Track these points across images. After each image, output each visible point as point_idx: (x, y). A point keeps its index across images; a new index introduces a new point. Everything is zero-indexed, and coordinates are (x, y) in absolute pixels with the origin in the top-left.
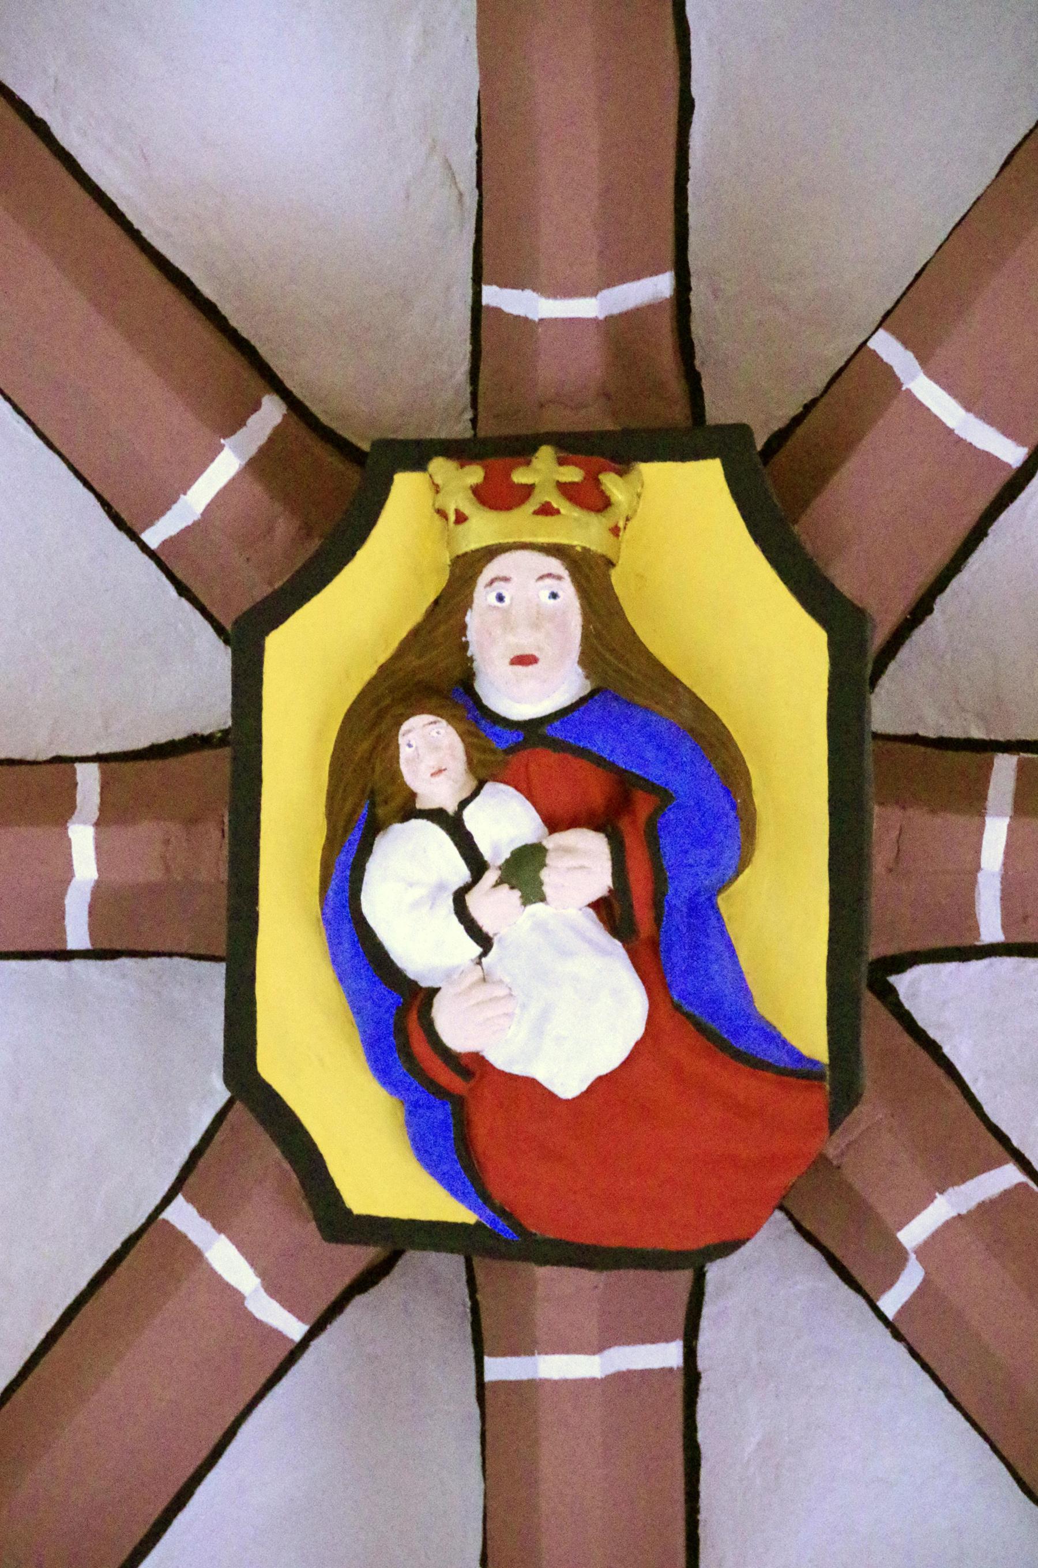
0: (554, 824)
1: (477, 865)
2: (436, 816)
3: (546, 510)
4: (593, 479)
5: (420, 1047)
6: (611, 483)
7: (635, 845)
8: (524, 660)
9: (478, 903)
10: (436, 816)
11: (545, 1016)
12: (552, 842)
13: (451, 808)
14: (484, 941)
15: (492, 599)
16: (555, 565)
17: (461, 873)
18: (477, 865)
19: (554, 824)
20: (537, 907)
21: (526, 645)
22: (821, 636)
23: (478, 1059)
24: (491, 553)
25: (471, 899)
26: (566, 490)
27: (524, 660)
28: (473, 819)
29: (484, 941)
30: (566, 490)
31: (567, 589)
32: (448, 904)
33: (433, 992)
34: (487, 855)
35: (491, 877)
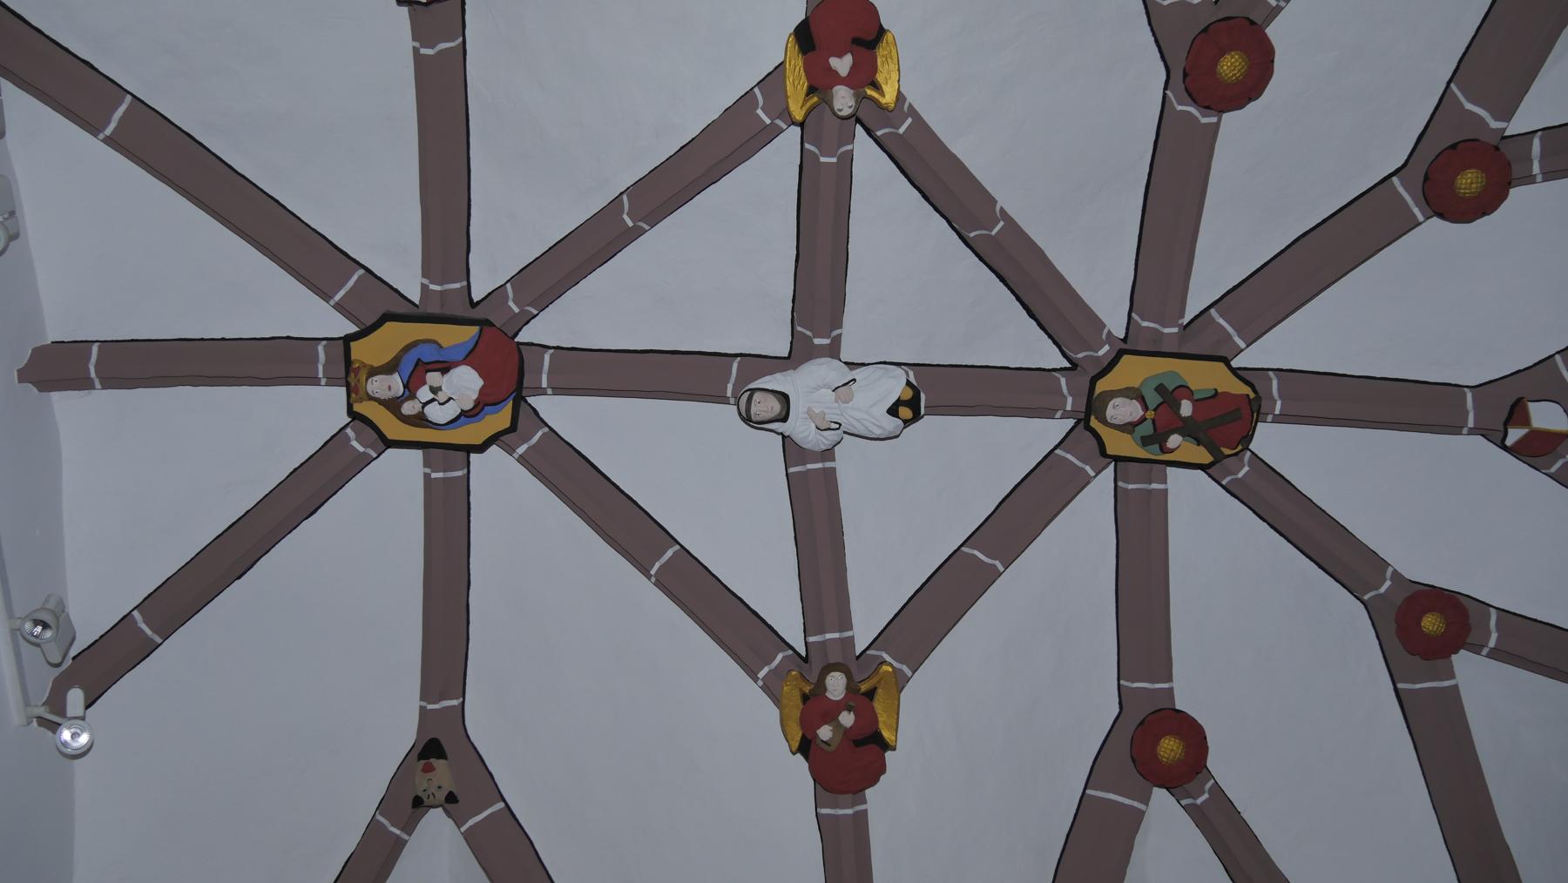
1: (433, 400)
2: (423, 408)
3: (359, 380)
5: (471, 413)
7: (429, 367)
8: (390, 388)
10: (423, 408)
14: (450, 399)
16: (370, 380)
17: (436, 403)
18: (433, 400)
20: (443, 388)
21: (386, 387)
22: (388, 323)
23: (475, 401)
25: (441, 402)
26: (356, 376)
27: (390, 388)
29: (450, 399)
30: (356, 376)
31: (375, 378)
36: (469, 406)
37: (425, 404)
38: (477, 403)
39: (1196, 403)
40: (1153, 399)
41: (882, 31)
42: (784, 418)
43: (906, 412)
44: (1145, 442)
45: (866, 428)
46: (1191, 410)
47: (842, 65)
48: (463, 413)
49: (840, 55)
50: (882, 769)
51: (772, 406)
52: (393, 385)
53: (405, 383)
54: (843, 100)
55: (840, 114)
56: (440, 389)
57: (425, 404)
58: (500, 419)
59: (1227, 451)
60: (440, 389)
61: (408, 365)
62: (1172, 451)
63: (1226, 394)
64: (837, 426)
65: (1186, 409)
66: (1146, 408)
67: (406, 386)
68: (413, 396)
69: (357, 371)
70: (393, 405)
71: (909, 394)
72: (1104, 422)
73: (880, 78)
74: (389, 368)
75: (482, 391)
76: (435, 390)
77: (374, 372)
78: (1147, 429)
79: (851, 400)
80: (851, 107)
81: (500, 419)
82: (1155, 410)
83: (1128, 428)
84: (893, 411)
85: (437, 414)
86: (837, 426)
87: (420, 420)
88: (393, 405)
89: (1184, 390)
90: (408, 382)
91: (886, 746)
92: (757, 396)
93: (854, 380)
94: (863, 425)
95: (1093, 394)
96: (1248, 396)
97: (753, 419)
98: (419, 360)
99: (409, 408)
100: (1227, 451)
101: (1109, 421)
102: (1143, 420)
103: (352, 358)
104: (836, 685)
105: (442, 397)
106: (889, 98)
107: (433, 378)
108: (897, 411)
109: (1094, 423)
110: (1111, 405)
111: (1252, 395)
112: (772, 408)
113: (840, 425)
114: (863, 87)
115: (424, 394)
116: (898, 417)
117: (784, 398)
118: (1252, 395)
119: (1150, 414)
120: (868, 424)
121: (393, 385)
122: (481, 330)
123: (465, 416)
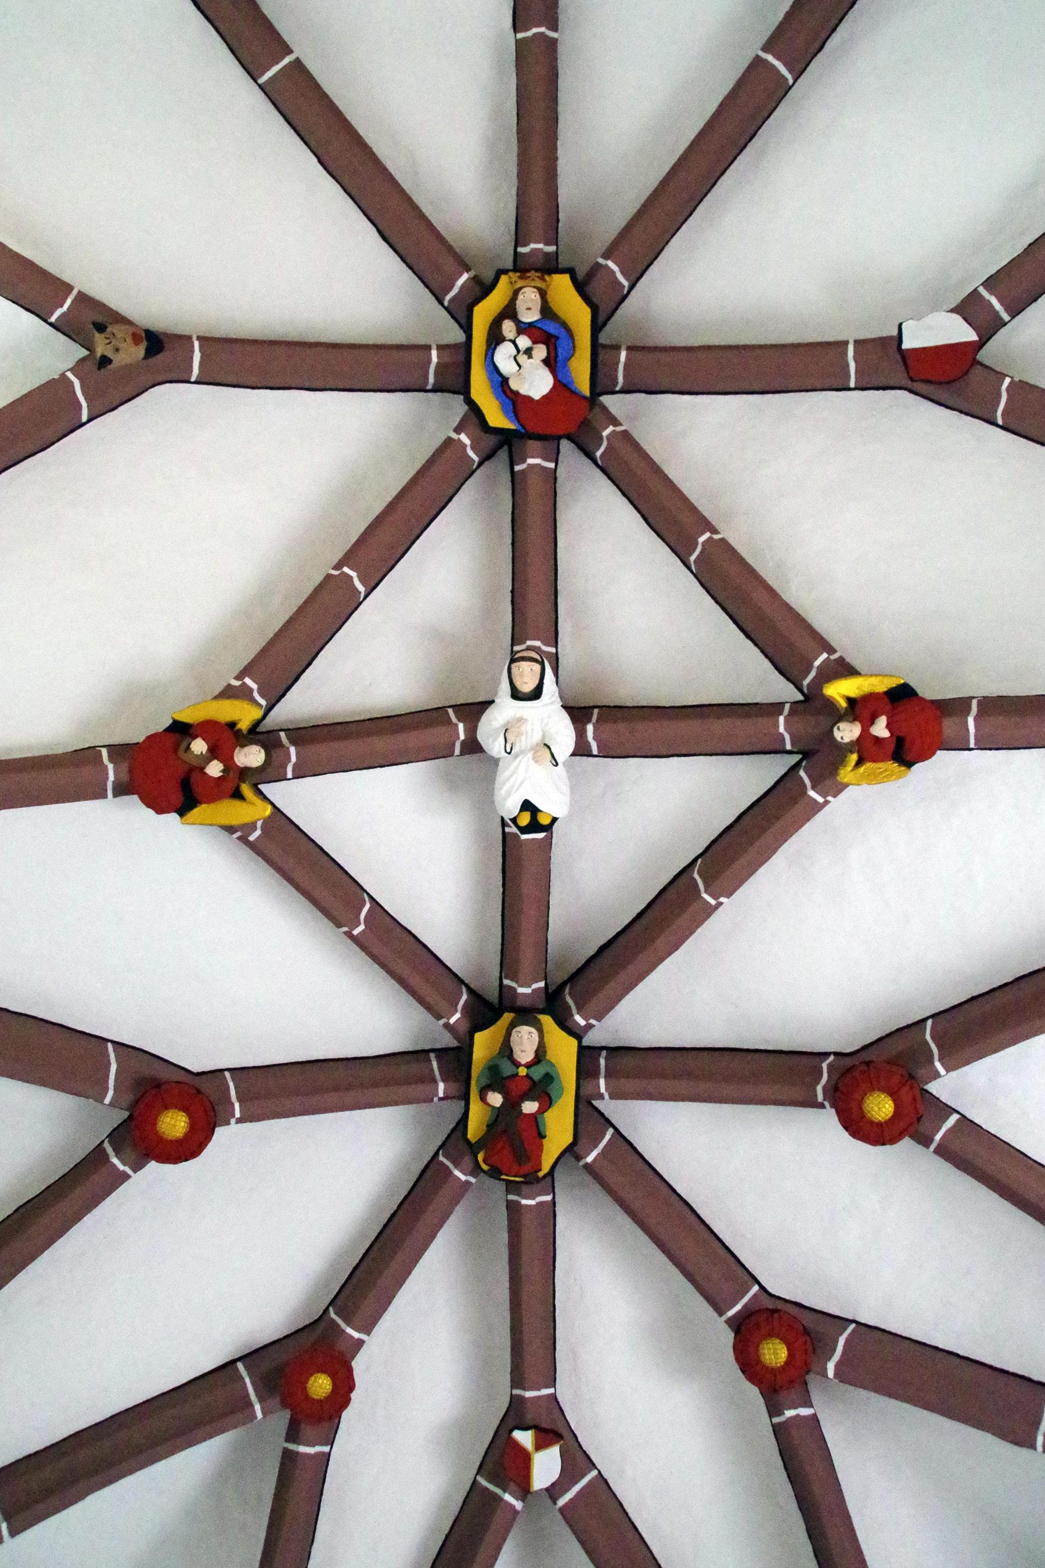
0: (535, 342)
1: (518, 351)
2: (510, 341)
3: (533, 280)
4: (543, 276)
6: (547, 277)
7: (552, 348)
8: (529, 309)
9: (519, 358)
10: (510, 341)
11: (532, 383)
12: (535, 346)
13: (513, 339)
14: (520, 366)
15: (522, 296)
16: (535, 290)
17: (515, 352)
18: (518, 351)
19: (535, 342)
20: (531, 360)
21: (530, 305)
24: (520, 289)
26: (538, 277)
27: (529, 309)
28: (518, 341)
29: (520, 366)
31: (538, 295)
32: (513, 358)
33: (508, 378)
34: (520, 348)
35: (521, 353)
36: (514, 385)
37: (514, 342)
38: (517, 394)
39: (534, 1118)
40: (537, 1073)
41: (909, 764)
42: (516, 695)
43: (525, 819)
44: (493, 1069)
45: (508, 779)
46: (528, 1112)
47: (880, 729)
48: (505, 380)
49: (888, 726)
50: (160, 810)
51: (527, 685)
52: (529, 312)
53: (535, 324)
54: (847, 732)
55: (835, 729)
56: (530, 357)
57: (514, 342)
58: (497, 417)
59: (480, 1157)
60: (530, 357)
61: (551, 328)
62: (483, 1099)
63: (540, 1148)
64: (508, 750)
65: (530, 1107)
66: (528, 1066)
67: (530, 324)
68: (520, 332)
69: (543, 279)
70: (509, 312)
71: (544, 821)
72: (513, 1025)
73: (868, 766)
74: (547, 311)
75: (528, 399)
76: (528, 352)
77: (543, 294)
78: (507, 1069)
79: (536, 762)
80: (842, 738)
81: (497, 417)
82: (527, 1076)
83: (506, 1050)
84: (527, 806)
85: (504, 358)
86: (508, 750)
87: (495, 338)
88: (509, 312)
89: (547, 1102)
90: (535, 327)
91: (182, 812)
92: (537, 667)
93: (557, 764)
94: (511, 776)
95: (538, 1013)
96: (540, 1170)
97: (513, 666)
98: (557, 338)
99: (508, 328)
100: (480, 1157)
101: (514, 1030)
102: (517, 1065)
103: (553, 275)
104: (252, 757)
105: (522, 358)
106: (846, 774)
108: (527, 810)
109: (508, 1017)
110: (533, 1030)
111: (541, 1174)
112: (526, 683)
113: (509, 753)
114: (858, 752)
115: (524, 342)
116: (521, 810)
117: (536, 694)
118: (541, 1174)
119: (523, 1071)
120: (512, 780)
121: (529, 312)
122: (584, 398)
123: (502, 382)
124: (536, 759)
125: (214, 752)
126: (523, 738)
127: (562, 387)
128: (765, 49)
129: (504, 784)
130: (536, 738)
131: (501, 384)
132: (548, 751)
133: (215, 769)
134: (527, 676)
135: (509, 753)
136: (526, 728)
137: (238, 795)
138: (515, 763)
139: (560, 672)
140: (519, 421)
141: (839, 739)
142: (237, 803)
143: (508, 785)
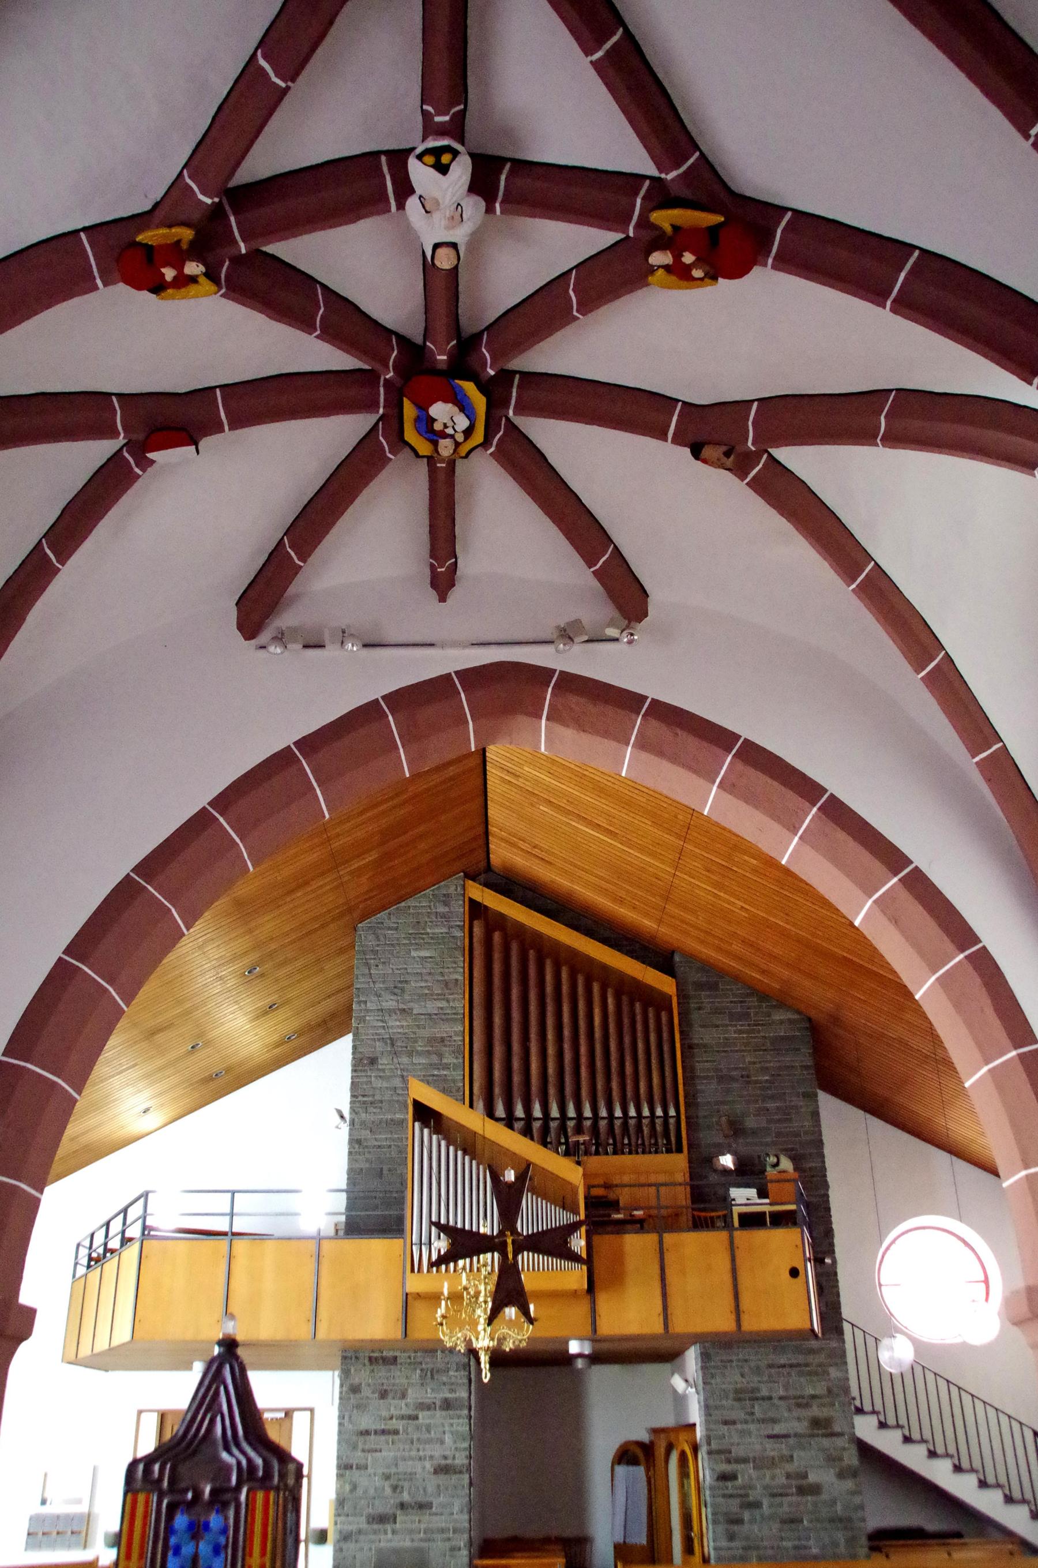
42: (454, 246)
43: (445, 159)
49: (164, 275)
57: (455, 431)
71: (430, 159)
76: (445, 426)
84: (443, 169)
86: (459, 207)
87: (468, 432)
88: (457, 445)
99: (460, 438)
107: (438, 427)
113: (459, 204)
115: (450, 431)
117: (436, 246)
121: (443, 443)
124: (437, 203)
125: (689, 268)
126: (448, 215)
127: (423, 407)
128: (301, 567)
129: (462, 185)
130: (436, 216)
131: (464, 406)
132: (427, 209)
133: (688, 258)
134: (445, 260)
135: (459, 204)
136: (443, 223)
137: (675, 228)
138: (455, 199)
139: (421, 258)
140: (453, 388)
141: (200, 265)
142: (679, 223)
143: (460, 184)
